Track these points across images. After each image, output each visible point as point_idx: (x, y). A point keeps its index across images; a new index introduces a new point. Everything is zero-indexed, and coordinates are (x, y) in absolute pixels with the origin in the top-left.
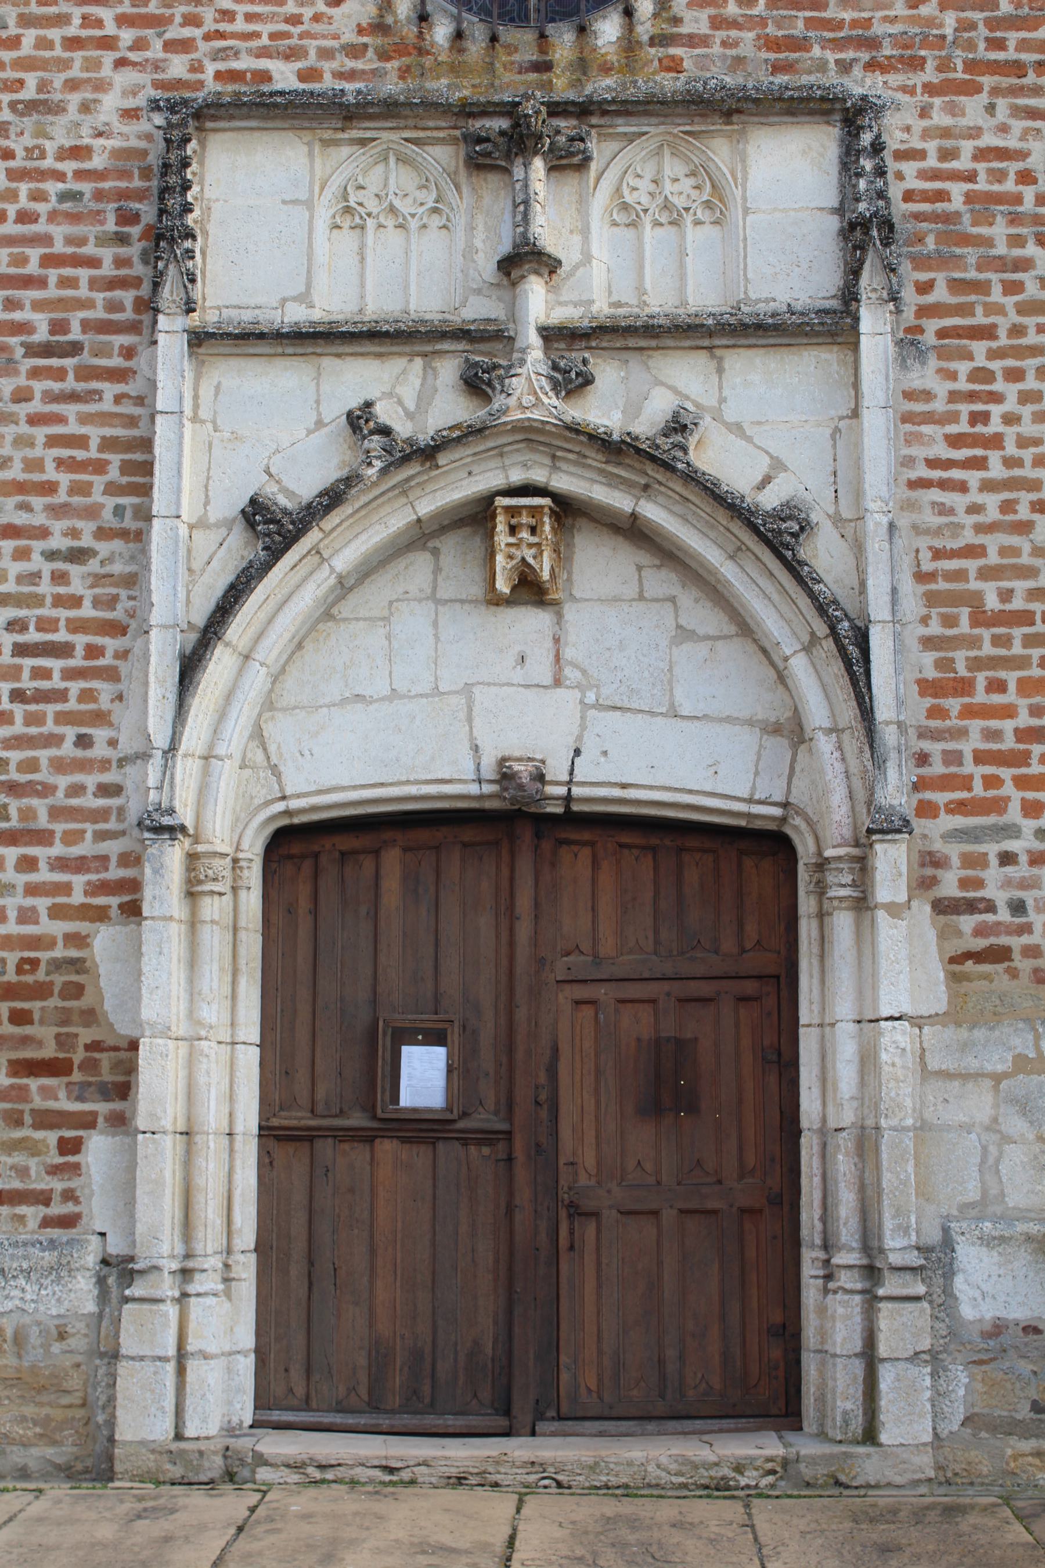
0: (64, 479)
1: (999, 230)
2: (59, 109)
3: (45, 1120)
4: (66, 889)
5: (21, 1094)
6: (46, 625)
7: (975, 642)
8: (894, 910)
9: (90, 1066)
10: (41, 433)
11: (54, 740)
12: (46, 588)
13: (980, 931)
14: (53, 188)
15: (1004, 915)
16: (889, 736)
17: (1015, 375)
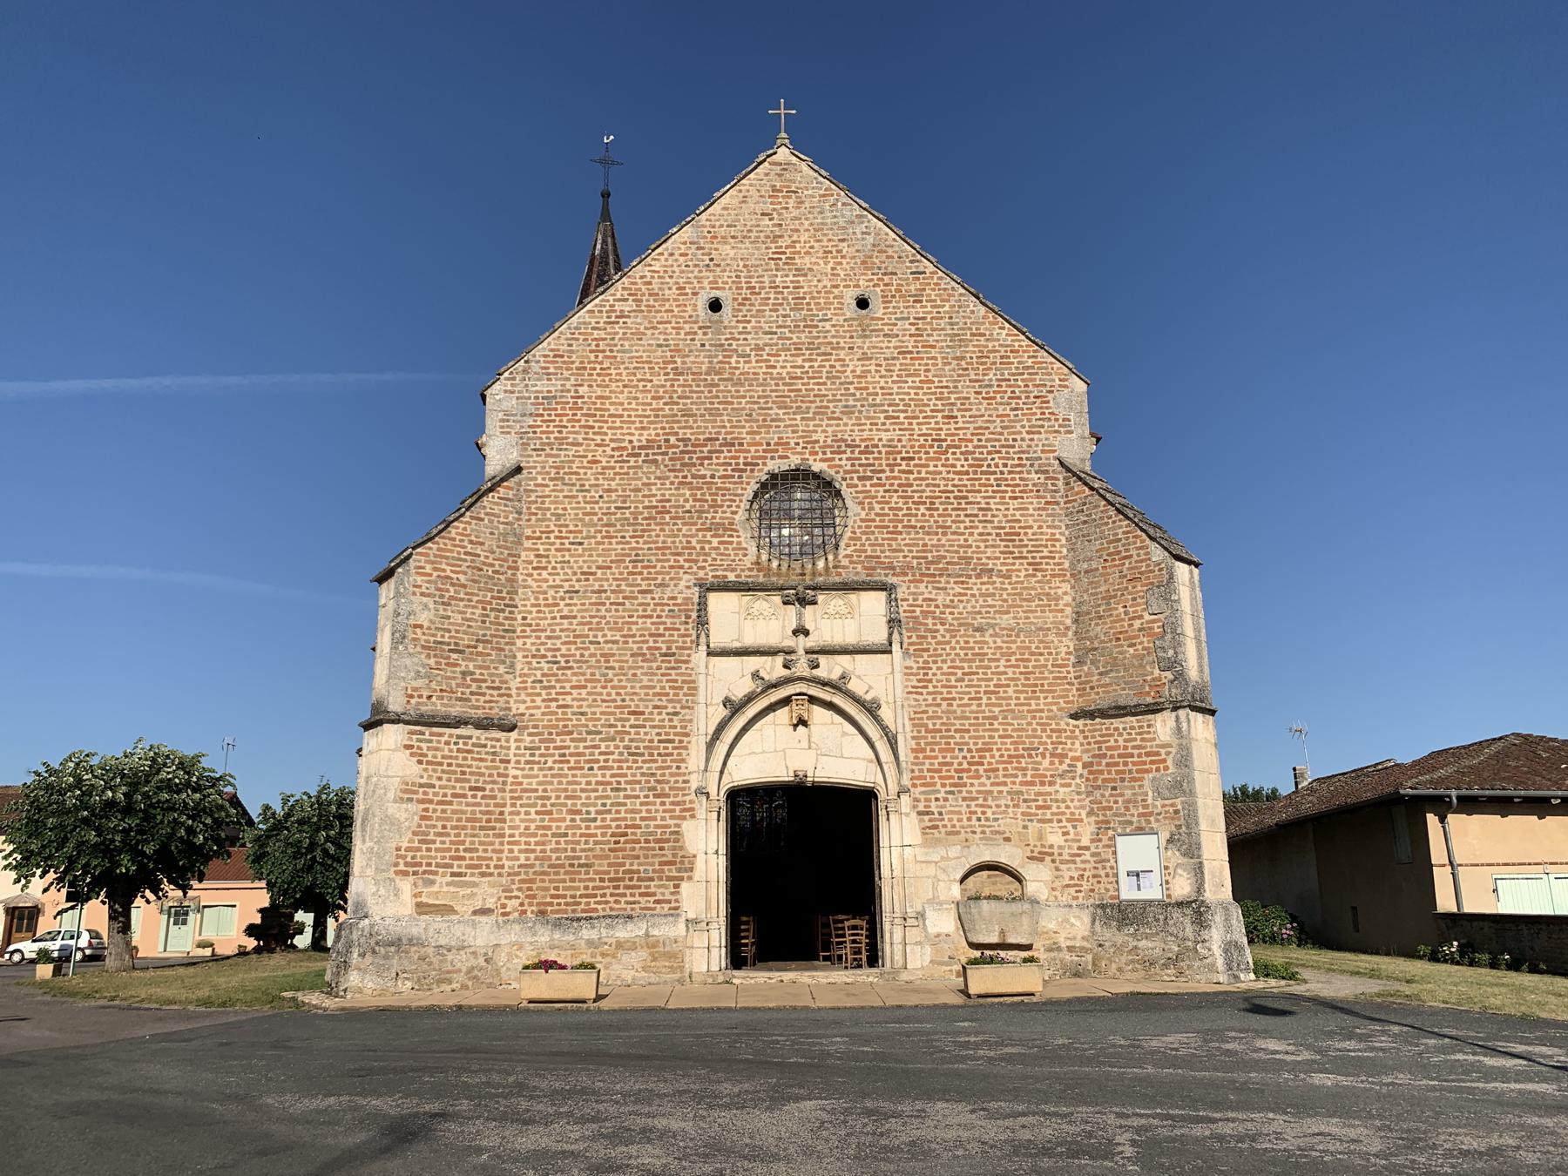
0: (672, 692)
1: (930, 621)
2: (668, 586)
3: (669, 879)
4: (674, 811)
5: (662, 871)
6: (667, 734)
7: (926, 738)
8: (907, 815)
9: (682, 862)
10: (665, 678)
11: (670, 767)
12: (666, 723)
13: (930, 820)
14: (667, 608)
15: (937, 816)
16: (903, 765)
17: (935, 662)
